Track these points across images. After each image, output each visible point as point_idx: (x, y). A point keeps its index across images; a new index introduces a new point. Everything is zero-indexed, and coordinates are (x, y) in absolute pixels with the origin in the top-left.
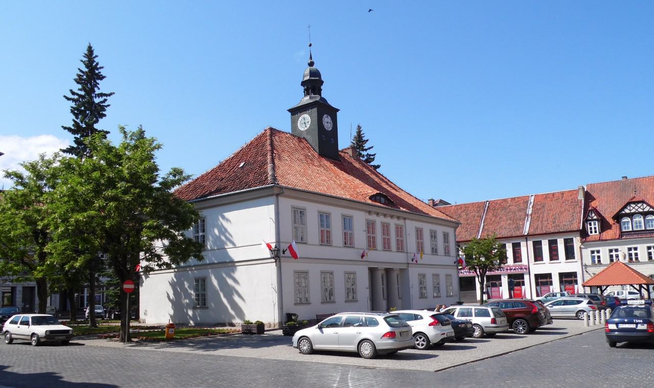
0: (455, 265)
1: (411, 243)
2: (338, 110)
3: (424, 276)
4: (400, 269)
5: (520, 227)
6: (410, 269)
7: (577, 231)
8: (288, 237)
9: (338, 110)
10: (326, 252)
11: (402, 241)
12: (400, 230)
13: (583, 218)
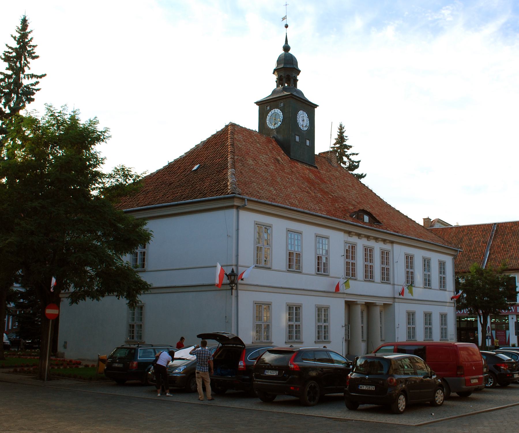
0: (452, 301)
2: (316, 106)
6: (396, 304)
9: (316, 106)
12: (385, 256)
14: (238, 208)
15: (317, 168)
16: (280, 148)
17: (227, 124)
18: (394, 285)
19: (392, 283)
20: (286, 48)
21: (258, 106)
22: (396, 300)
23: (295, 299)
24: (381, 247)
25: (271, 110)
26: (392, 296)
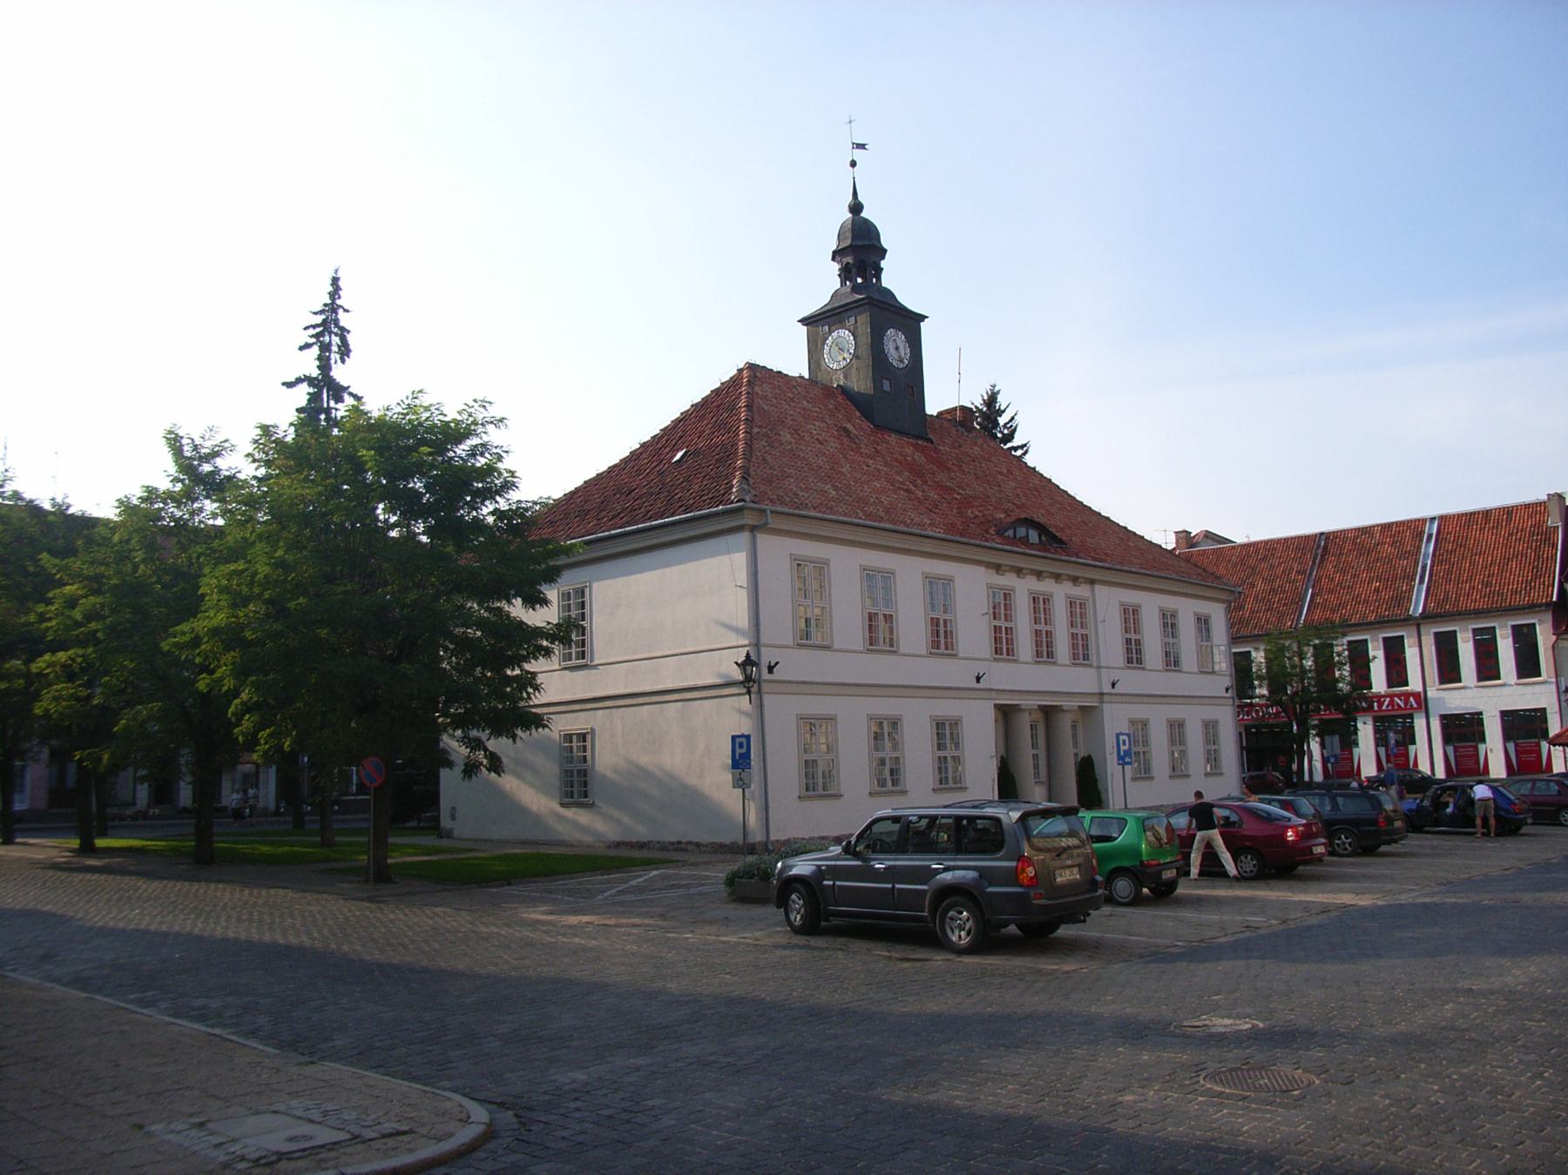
0: (1229, 695)
1: (1109, 640)
2: (923, 318)
3: (1145, 724)
4: (1080, 707)
5: (1403, 599)
6: (1106, 707)
7: (1549, 605)
8: (780, 626)
9: (923, 318)
10: (881, 668)
11: (1085, 637)
12: (1078, 610)
13: (1560, 574)
14: (753, 529)
15: (932, 442)
17: (741, 366)
18: (1099, 667)
19: (1095, 664)
20: (856, 208)
21: (805, 328)
23: (885, 707)
25: (830, 332)
26: (1096, 691)
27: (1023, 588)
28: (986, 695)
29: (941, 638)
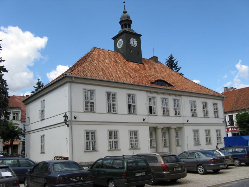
2: (141, 35)
9: (141, 35)
15: (143, 64)
16: (122, 57)
21: (113, 40)
22: (185, 125)
24: (190, 99)
25: (118, 41)
27: (159, 98)
28: (147, 124)
29: (131, 109)
